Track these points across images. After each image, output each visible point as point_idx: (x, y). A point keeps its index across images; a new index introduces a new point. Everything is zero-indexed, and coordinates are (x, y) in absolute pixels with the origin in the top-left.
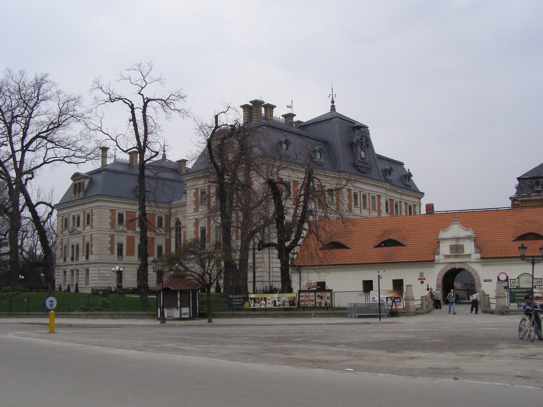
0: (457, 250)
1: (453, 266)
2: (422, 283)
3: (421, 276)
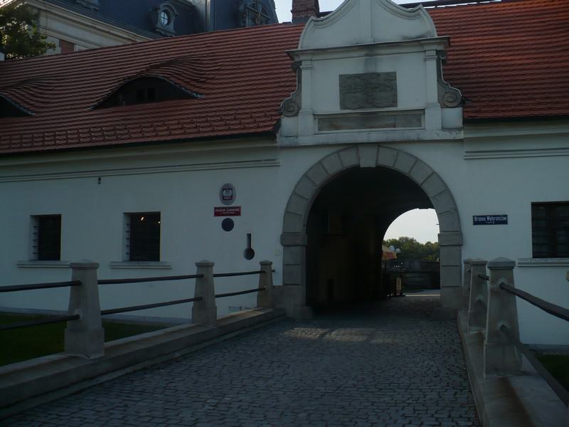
0: (368, 94)
1: (349, 160)
2: (228, 226)
3: (224, 199)
